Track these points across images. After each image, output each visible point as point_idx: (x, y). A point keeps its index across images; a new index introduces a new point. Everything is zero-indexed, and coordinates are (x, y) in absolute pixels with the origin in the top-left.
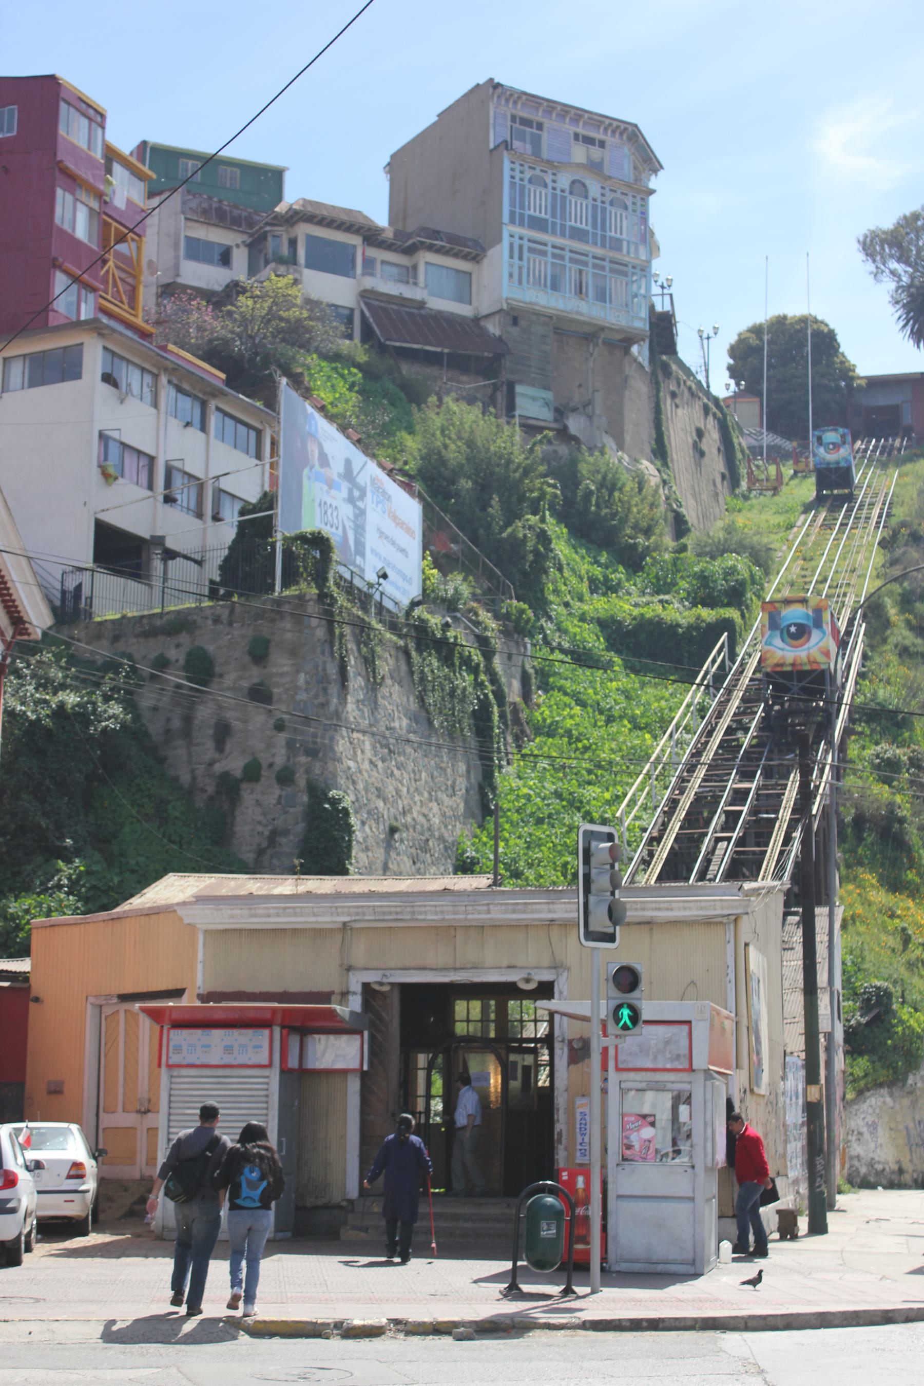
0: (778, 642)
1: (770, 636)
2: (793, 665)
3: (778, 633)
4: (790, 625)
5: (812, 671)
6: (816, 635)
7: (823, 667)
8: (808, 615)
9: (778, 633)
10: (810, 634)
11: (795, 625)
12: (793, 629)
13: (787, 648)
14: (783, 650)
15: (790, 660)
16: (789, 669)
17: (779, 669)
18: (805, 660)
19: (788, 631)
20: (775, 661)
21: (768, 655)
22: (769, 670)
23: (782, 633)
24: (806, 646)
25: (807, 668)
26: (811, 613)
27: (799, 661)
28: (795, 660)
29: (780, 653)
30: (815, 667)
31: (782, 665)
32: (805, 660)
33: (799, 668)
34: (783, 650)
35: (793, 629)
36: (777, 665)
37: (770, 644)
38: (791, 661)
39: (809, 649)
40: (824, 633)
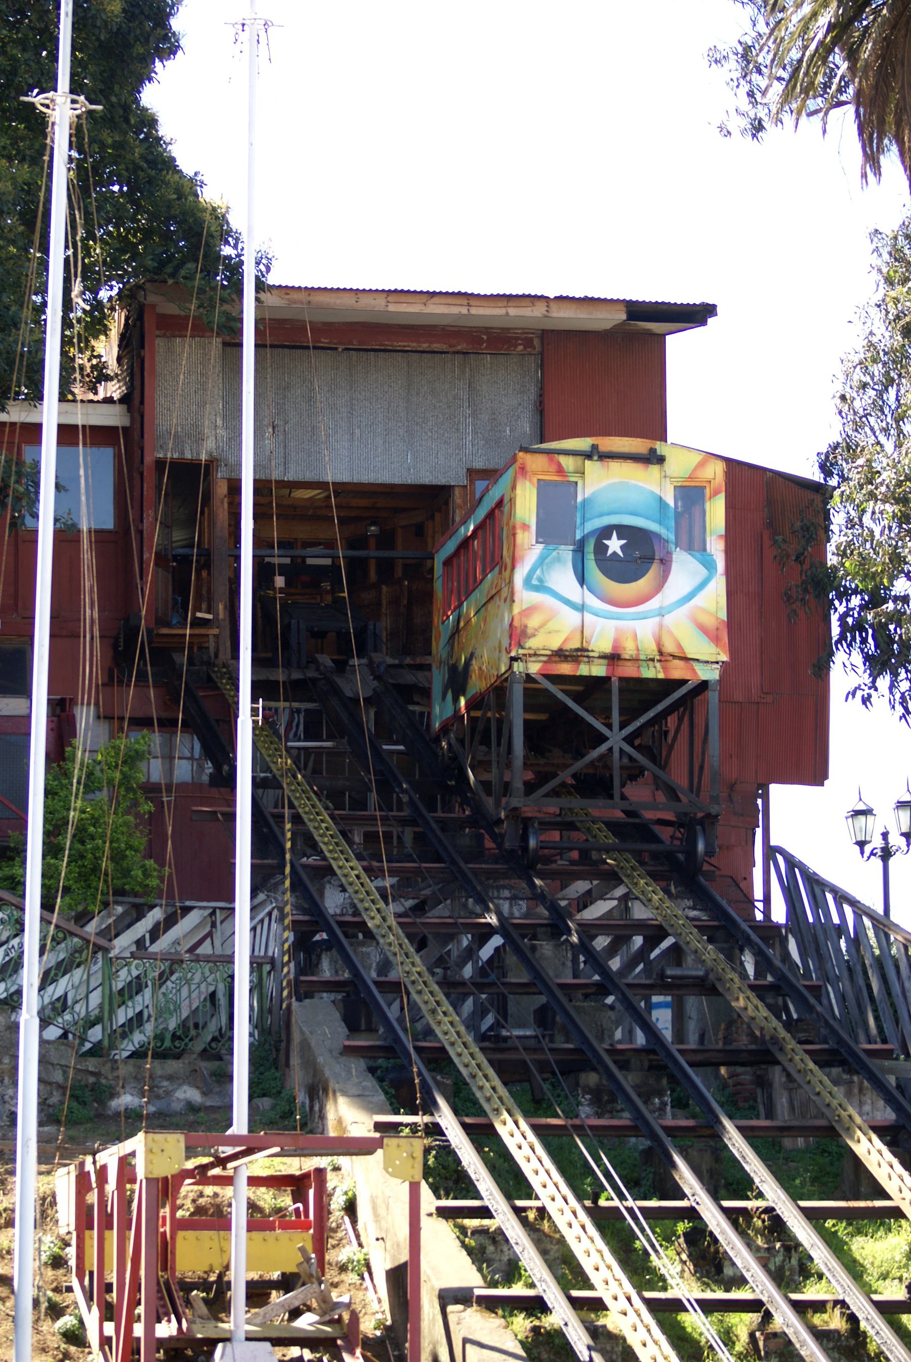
0: (563, 579)
1: (541, 561)
2: (613, 658)
4: (606, 532)
6: (684, 571)
9: (567, 553)
10: (666, 563)
11: (623, 531)
12: (615, 545)
13: (593, 601)
15: (602, 644)
16: (599, 670)
17: (565, 669)
18: (650, 648)
19: (600, 549)
20: (555, 646)
21: (533, 623)
22: (534, 668)
23: (580, 549)
24: (653, 604)
25: (649, 673)
26: (671, 503)
27: (629, 650)
28: (616, 644)
29: (569, 619)
30: (678, 671)
31: (579, 654)
32: (650, 648)
33: (629, 671)
34: (581, 608)
36: (560, 655)
37: (541, 587)
38: (607, 648)
39: (661, 613)
40: (709, 565)
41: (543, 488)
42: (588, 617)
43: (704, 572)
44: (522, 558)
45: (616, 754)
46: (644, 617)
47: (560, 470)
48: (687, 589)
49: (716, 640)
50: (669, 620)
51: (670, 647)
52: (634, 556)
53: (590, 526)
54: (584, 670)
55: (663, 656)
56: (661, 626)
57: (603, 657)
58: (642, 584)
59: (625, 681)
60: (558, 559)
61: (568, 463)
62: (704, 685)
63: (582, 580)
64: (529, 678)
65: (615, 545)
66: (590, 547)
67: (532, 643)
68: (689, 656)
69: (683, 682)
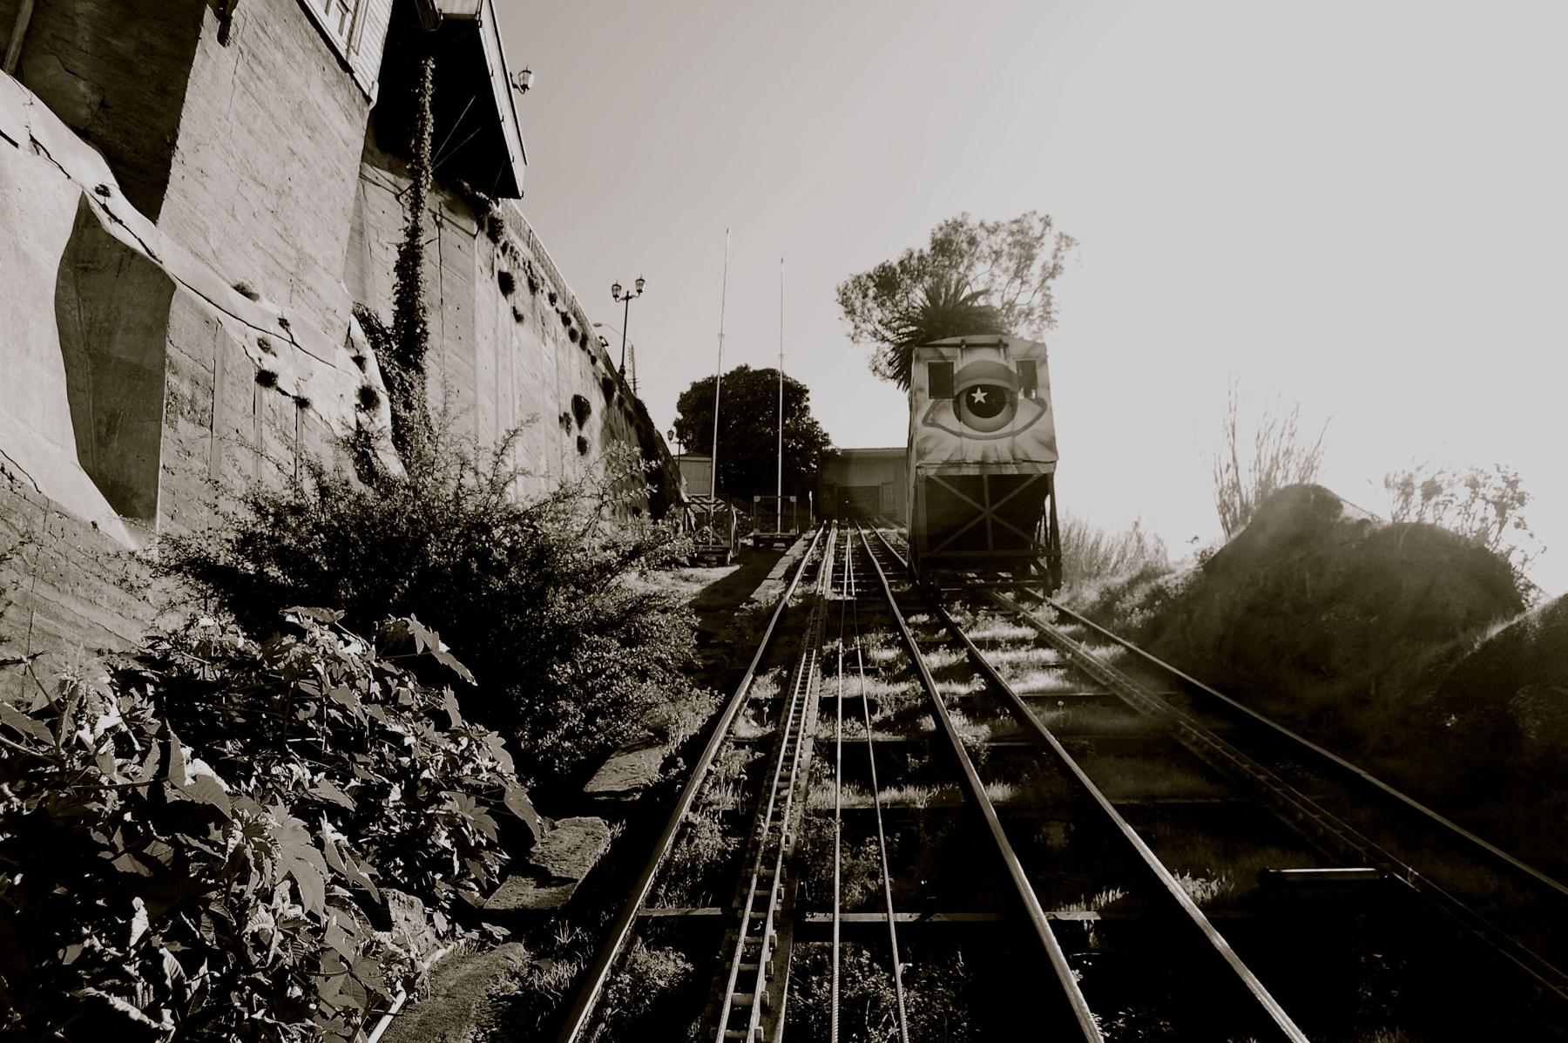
0: (948, 418)
1: (933, 408)
2: (982, 464)
3: (949, 402)
4: (974, 389)
5: (1024, 477)
7: (1043, 470)
8: (1007, 368)
9: (949, 402)
11: (984, 388)
16: (973, 471)
17: (953, 472)
18: (1007, 457)
19: (970, 400)
21: (930, 445)
22: (932, 472)
25: (1011, 470)
27: (992, 458)
30: (1027, 469)
33: (994, 471)
35: (979, 396)
36: (949, 463)
37: (934, 424)
39: (1013, 434)
41: (933, 369)
42: (965, 440)
43: (1038, 409)
45: (989, 523)
46: (1001, 437)
47: (942, 357)
48: (1029, 420)
50: (1018, 439)
51: (1020, 455)
53: (962, 387)
54: (966, 471)
55: (1016, 462)
60: (944, 407)
61: (945, 351)
64: (928, 480)
65: (979, 396)
67: (929, 458)
69: (1030, 476)
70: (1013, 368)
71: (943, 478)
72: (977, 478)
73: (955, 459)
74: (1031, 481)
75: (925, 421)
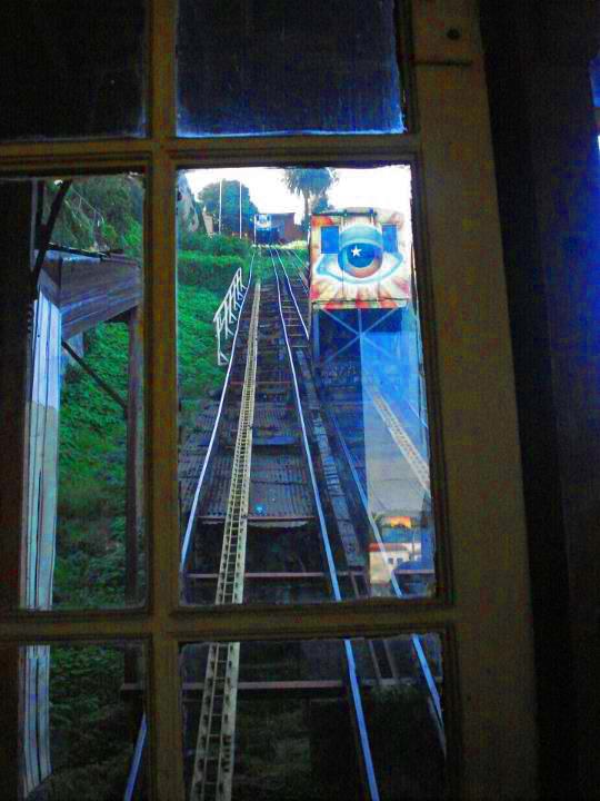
0: (334, 268)
1: (324, 261)
2: (357, 301)
3: (334, 256)
4: (352, 247)
5: (382, 311)
6: (388, 260)
8: (378, 234)
10: (379, 260)
11: (359, 246)
12: (356, 252)
13: (346, 275)
14: (342, 280)
15: (352, 295)
16: (351, 306)
17: (337, 307)
18: (375, 295)
21: (321, 287)
22: (322, 307)
25: (375, 306)
27: (364, 297)
28: (358, 295)
30: (388, 304)
31: (342, 301)
32: (375, 295)
33: (366, 306)
34: (342, 280)
35: (356, 252)
36: (332, 301)
38: (354, 296)
39: (379, 279)
40: (400, 258)
43: (396, 261)
44: (315, 260)
47: (331, 222)
49: (404, 288)
51: (383, 294)
52: (368, 257)
54: (346, 306)
55: (381, 299)
56: (379, 285)
57: (353, 300)
58: (369, 267)
59: (365, 311)
62: (400, 310)
63: (342, 269)
66: (345, 258)
68: (393, 296)
70: (380, 230)
71: (332, 311)
72: (354, 311)
73: (340, 296)
74: (388, 314)
75: (318, 270)
